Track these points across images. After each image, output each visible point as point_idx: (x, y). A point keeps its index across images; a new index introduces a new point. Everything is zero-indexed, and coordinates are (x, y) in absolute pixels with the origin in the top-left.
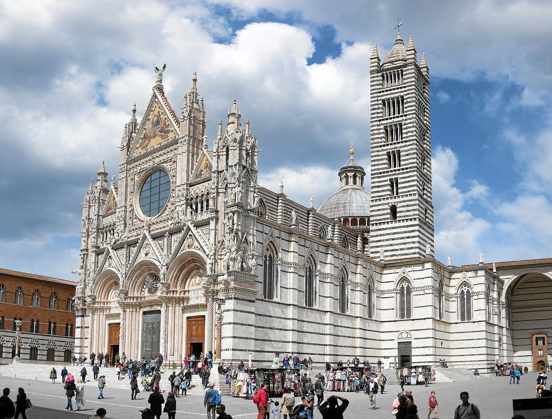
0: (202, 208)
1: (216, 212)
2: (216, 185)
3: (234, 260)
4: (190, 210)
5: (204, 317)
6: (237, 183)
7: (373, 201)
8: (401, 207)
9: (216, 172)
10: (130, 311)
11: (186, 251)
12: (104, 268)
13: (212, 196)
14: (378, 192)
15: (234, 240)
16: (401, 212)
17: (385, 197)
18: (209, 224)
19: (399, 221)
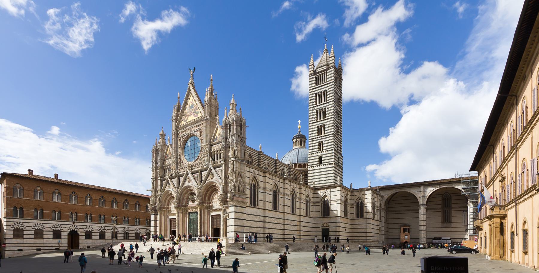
3: (235, 186)
6: (235, 145)
7: (309, 154)
8: (325, 157)
16: (325, 160)
17: (316, 152)
19: (324, 165)
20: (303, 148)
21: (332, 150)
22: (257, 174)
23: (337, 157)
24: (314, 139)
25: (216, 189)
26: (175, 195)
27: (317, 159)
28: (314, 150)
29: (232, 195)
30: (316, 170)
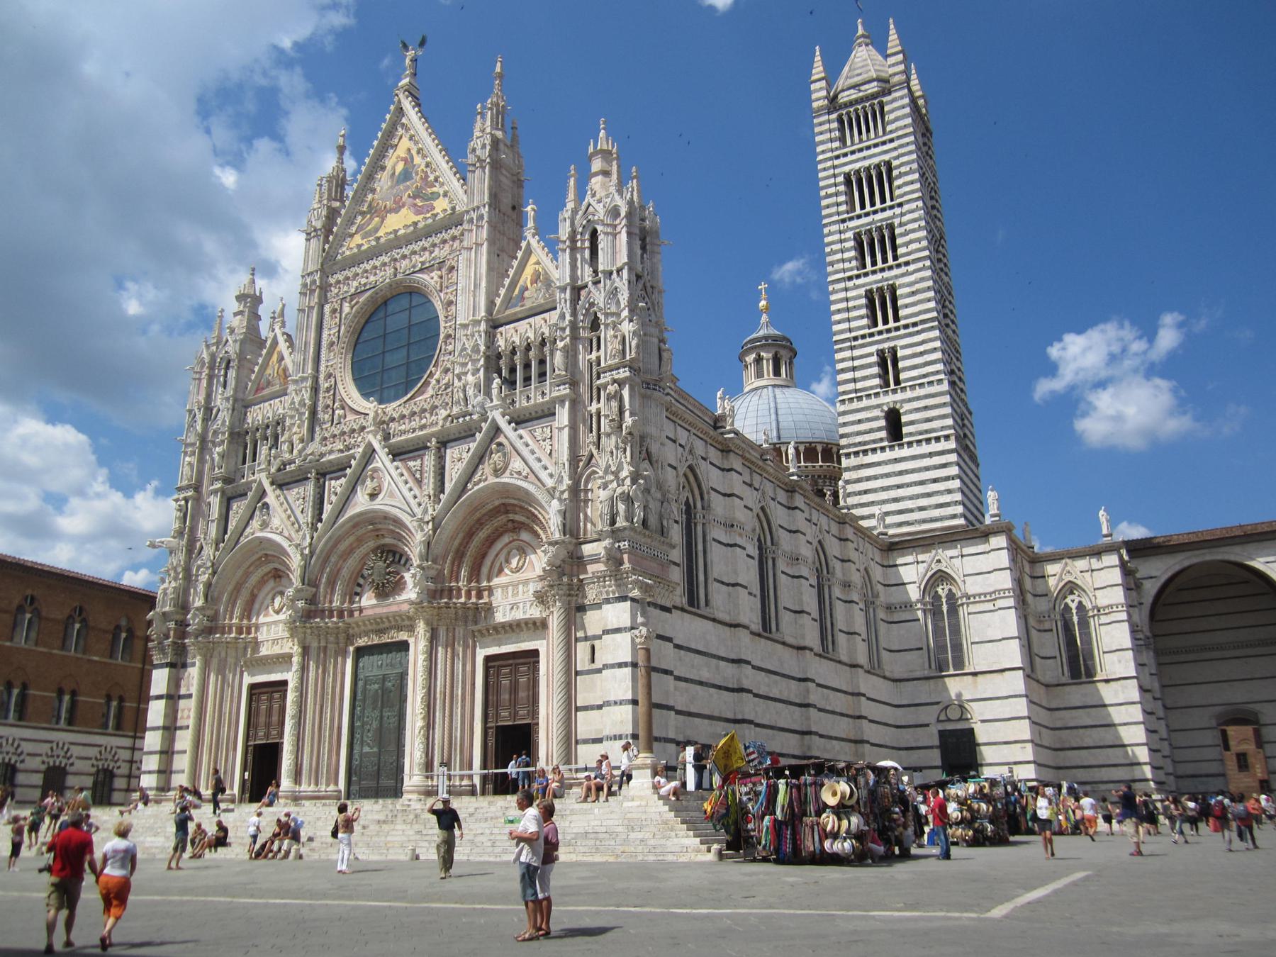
0: (527, 380)
1: (570, 385)
2: (568, 317)
3: (628, 499)
4: (497, 381)
5: (535, 653)
6: (625, 313)
7: (843, 401)
8: (911, 411)
9: (569, 288)
10: (319, 648)
11: (486, 483)
12: (246, 533)
13: (560, 344)
14: (854, 380)
15: (625, 450)
16: (912, 423)
18: (554, 414)
20: (788, 387)
21: (940, 381)
22: (702, 458)
23: (958, 410)
24: (855, 339)
25: (513, 521)
26: (295, 561)
27: (876, 418)
28: (859, 385)
29: (616, 545)
30: (879, 464)
